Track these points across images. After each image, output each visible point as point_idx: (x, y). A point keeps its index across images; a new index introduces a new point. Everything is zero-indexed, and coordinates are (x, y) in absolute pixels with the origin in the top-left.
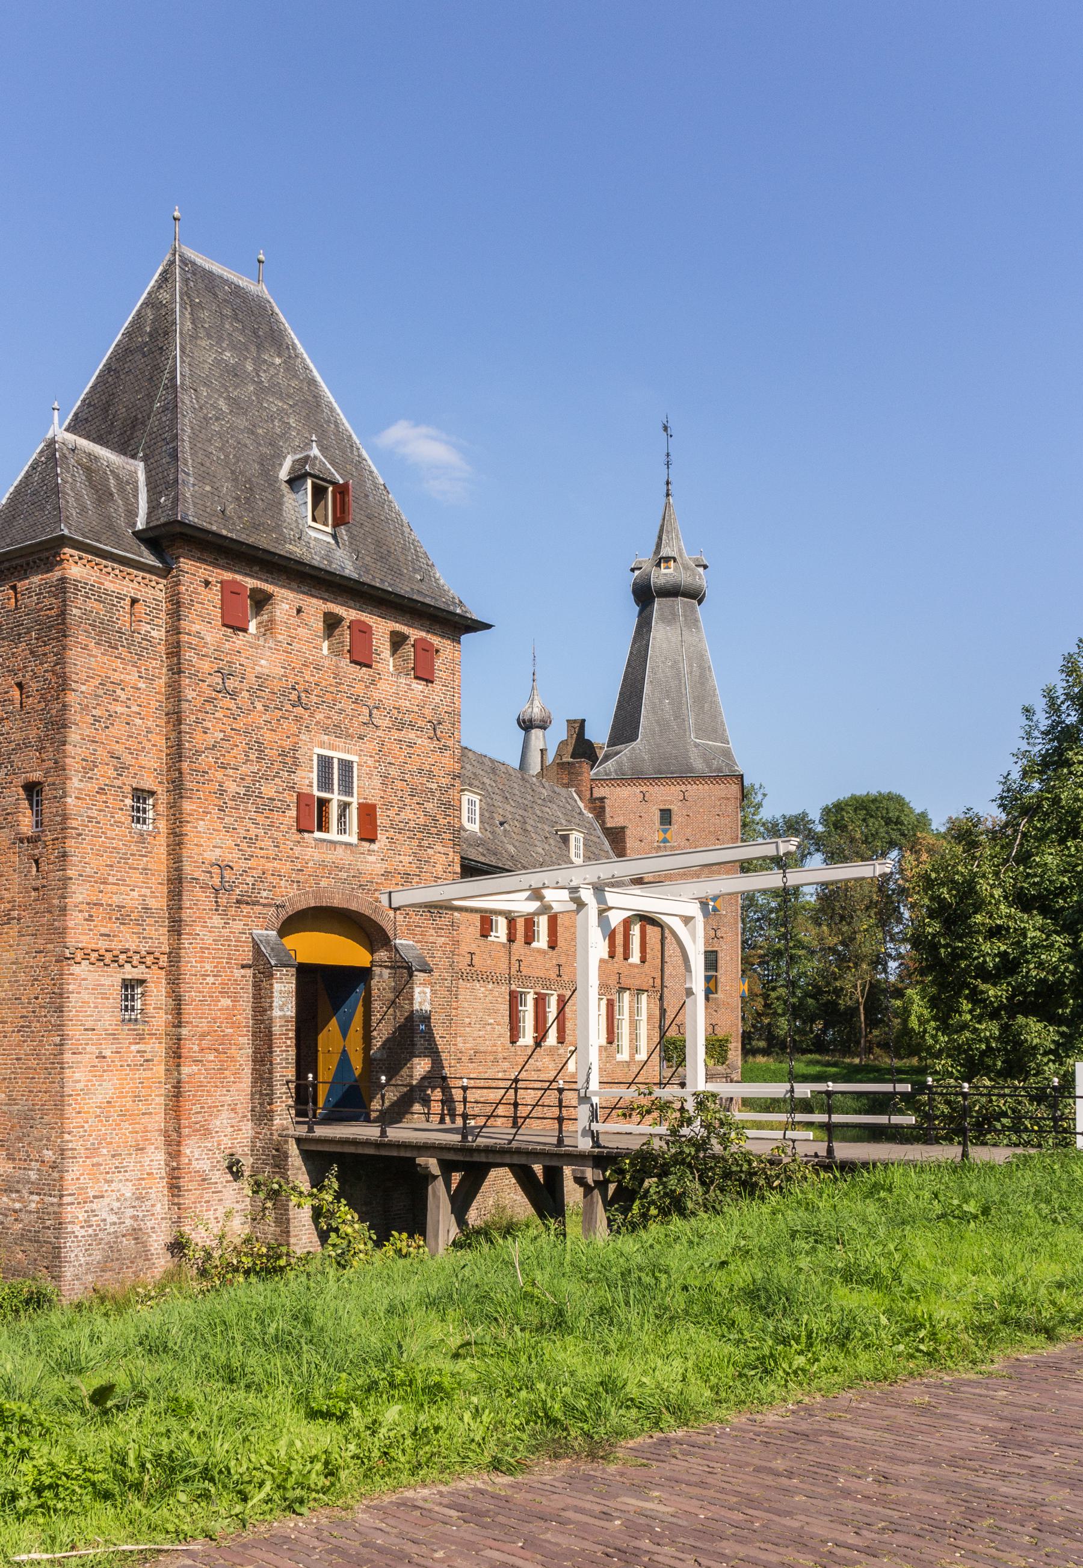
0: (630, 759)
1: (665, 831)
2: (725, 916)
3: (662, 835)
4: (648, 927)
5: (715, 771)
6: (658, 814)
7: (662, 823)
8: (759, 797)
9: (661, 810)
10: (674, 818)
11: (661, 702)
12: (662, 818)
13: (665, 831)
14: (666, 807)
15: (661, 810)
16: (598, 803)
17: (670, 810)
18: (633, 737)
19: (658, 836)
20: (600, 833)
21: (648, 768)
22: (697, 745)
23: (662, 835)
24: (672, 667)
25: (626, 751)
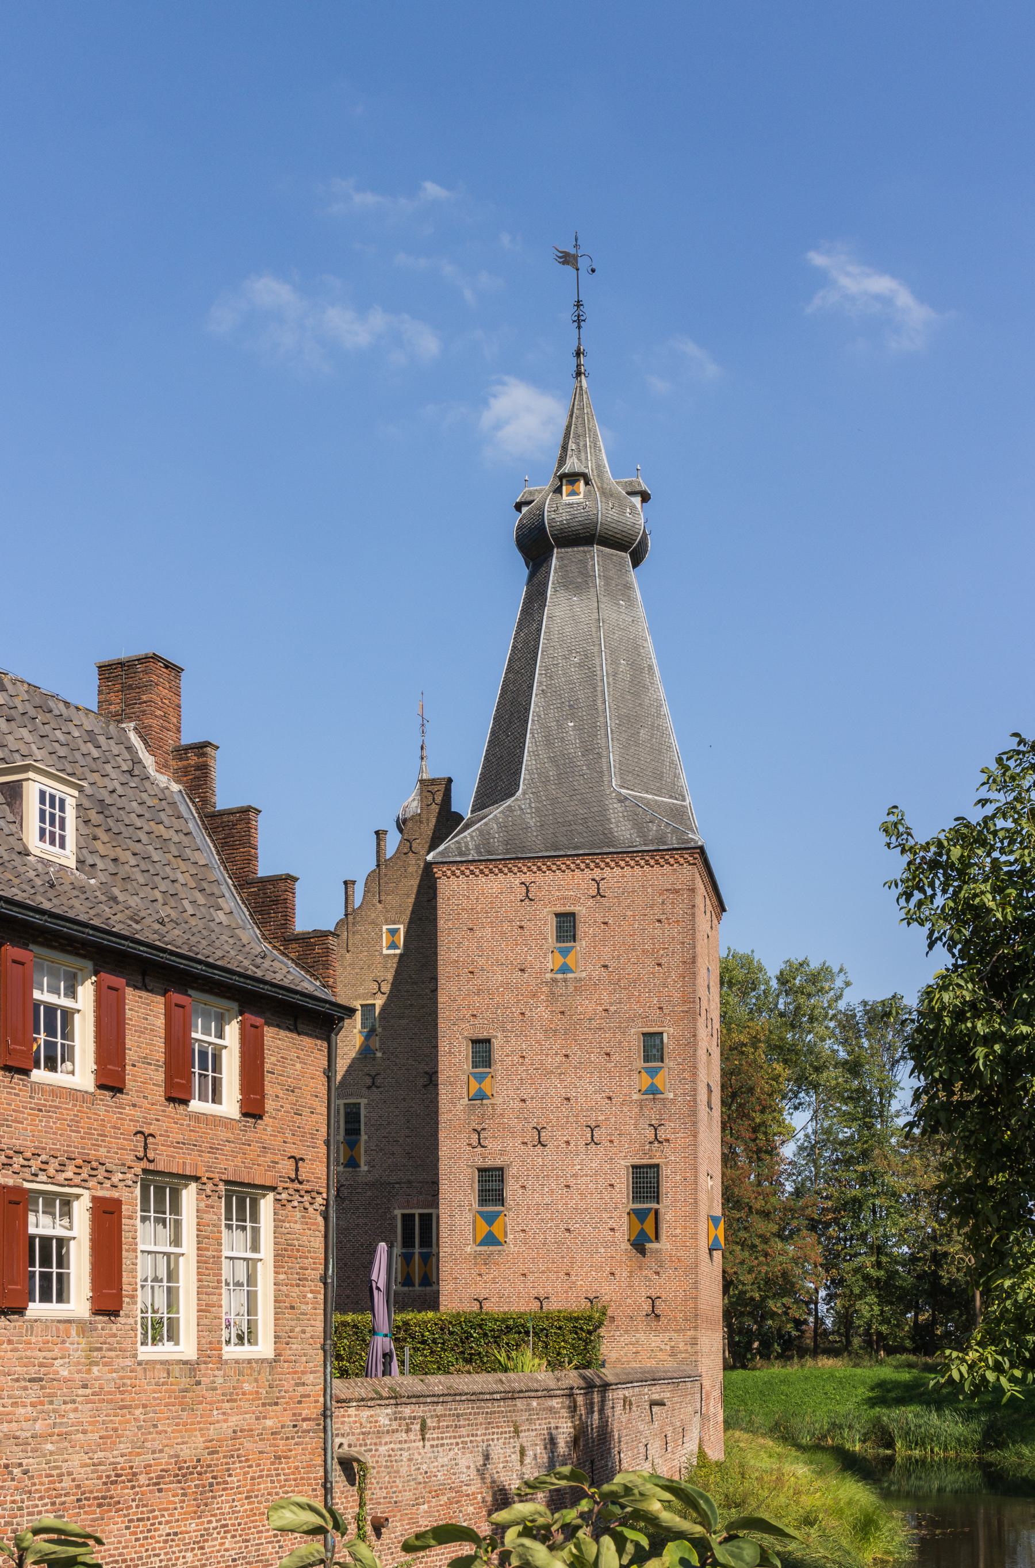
0: (503, 827)
1: (564, 953)
2: (673, 1101)
3: (560, 960)
4: (270, 1034)
5: (652, 842)
6: (552, 922)
7: (560, 938)
8: (839, 983)
9: (557, 915)
10: (581, 929)
11: (560, 726)
12: (559, 928)
13: (564, 953)
14: (568, 909)
15: (557, 915)
16: (193, 759)
17: (573, 915)
18: (510, 791)
19: (552, 962)
20: (194, 826)
21: (535, 841)
22: (622, 799)
23: (560, 960)
24: (580, 665)
25: (496, 812)
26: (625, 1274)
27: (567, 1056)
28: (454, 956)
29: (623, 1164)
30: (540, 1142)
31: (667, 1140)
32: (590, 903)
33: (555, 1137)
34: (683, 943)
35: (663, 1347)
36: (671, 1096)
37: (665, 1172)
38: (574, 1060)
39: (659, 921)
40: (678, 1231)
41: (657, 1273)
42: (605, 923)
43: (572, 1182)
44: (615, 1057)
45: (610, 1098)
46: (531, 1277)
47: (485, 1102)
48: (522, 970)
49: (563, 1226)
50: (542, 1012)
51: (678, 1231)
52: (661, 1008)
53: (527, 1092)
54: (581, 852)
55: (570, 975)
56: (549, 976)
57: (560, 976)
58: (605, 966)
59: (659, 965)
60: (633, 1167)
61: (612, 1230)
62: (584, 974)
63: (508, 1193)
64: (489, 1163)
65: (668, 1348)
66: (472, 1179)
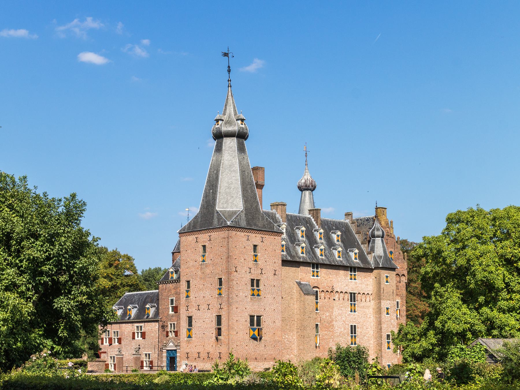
26: (215, 346)
36: (223, 296)
37: (222, 317)
38: (205, 286)
40: (225, 334)
41: (221, 346)
43: (205, 320)
44: (213, 285)
46: (197, 347)
47: (189, 298)
48: (196, 261)
49: (203, 333)
50: (199, 273)
51: (225, 334)
53: (196, 295)
54: (205, 229)
55: (205, 263)
56: (201, 263)
57: (203, 263)
58: (211, 260)
60: (217, 316)
62: (207, 262)
63: (193, 323)
64: (190, 315)
66: (186, 320)
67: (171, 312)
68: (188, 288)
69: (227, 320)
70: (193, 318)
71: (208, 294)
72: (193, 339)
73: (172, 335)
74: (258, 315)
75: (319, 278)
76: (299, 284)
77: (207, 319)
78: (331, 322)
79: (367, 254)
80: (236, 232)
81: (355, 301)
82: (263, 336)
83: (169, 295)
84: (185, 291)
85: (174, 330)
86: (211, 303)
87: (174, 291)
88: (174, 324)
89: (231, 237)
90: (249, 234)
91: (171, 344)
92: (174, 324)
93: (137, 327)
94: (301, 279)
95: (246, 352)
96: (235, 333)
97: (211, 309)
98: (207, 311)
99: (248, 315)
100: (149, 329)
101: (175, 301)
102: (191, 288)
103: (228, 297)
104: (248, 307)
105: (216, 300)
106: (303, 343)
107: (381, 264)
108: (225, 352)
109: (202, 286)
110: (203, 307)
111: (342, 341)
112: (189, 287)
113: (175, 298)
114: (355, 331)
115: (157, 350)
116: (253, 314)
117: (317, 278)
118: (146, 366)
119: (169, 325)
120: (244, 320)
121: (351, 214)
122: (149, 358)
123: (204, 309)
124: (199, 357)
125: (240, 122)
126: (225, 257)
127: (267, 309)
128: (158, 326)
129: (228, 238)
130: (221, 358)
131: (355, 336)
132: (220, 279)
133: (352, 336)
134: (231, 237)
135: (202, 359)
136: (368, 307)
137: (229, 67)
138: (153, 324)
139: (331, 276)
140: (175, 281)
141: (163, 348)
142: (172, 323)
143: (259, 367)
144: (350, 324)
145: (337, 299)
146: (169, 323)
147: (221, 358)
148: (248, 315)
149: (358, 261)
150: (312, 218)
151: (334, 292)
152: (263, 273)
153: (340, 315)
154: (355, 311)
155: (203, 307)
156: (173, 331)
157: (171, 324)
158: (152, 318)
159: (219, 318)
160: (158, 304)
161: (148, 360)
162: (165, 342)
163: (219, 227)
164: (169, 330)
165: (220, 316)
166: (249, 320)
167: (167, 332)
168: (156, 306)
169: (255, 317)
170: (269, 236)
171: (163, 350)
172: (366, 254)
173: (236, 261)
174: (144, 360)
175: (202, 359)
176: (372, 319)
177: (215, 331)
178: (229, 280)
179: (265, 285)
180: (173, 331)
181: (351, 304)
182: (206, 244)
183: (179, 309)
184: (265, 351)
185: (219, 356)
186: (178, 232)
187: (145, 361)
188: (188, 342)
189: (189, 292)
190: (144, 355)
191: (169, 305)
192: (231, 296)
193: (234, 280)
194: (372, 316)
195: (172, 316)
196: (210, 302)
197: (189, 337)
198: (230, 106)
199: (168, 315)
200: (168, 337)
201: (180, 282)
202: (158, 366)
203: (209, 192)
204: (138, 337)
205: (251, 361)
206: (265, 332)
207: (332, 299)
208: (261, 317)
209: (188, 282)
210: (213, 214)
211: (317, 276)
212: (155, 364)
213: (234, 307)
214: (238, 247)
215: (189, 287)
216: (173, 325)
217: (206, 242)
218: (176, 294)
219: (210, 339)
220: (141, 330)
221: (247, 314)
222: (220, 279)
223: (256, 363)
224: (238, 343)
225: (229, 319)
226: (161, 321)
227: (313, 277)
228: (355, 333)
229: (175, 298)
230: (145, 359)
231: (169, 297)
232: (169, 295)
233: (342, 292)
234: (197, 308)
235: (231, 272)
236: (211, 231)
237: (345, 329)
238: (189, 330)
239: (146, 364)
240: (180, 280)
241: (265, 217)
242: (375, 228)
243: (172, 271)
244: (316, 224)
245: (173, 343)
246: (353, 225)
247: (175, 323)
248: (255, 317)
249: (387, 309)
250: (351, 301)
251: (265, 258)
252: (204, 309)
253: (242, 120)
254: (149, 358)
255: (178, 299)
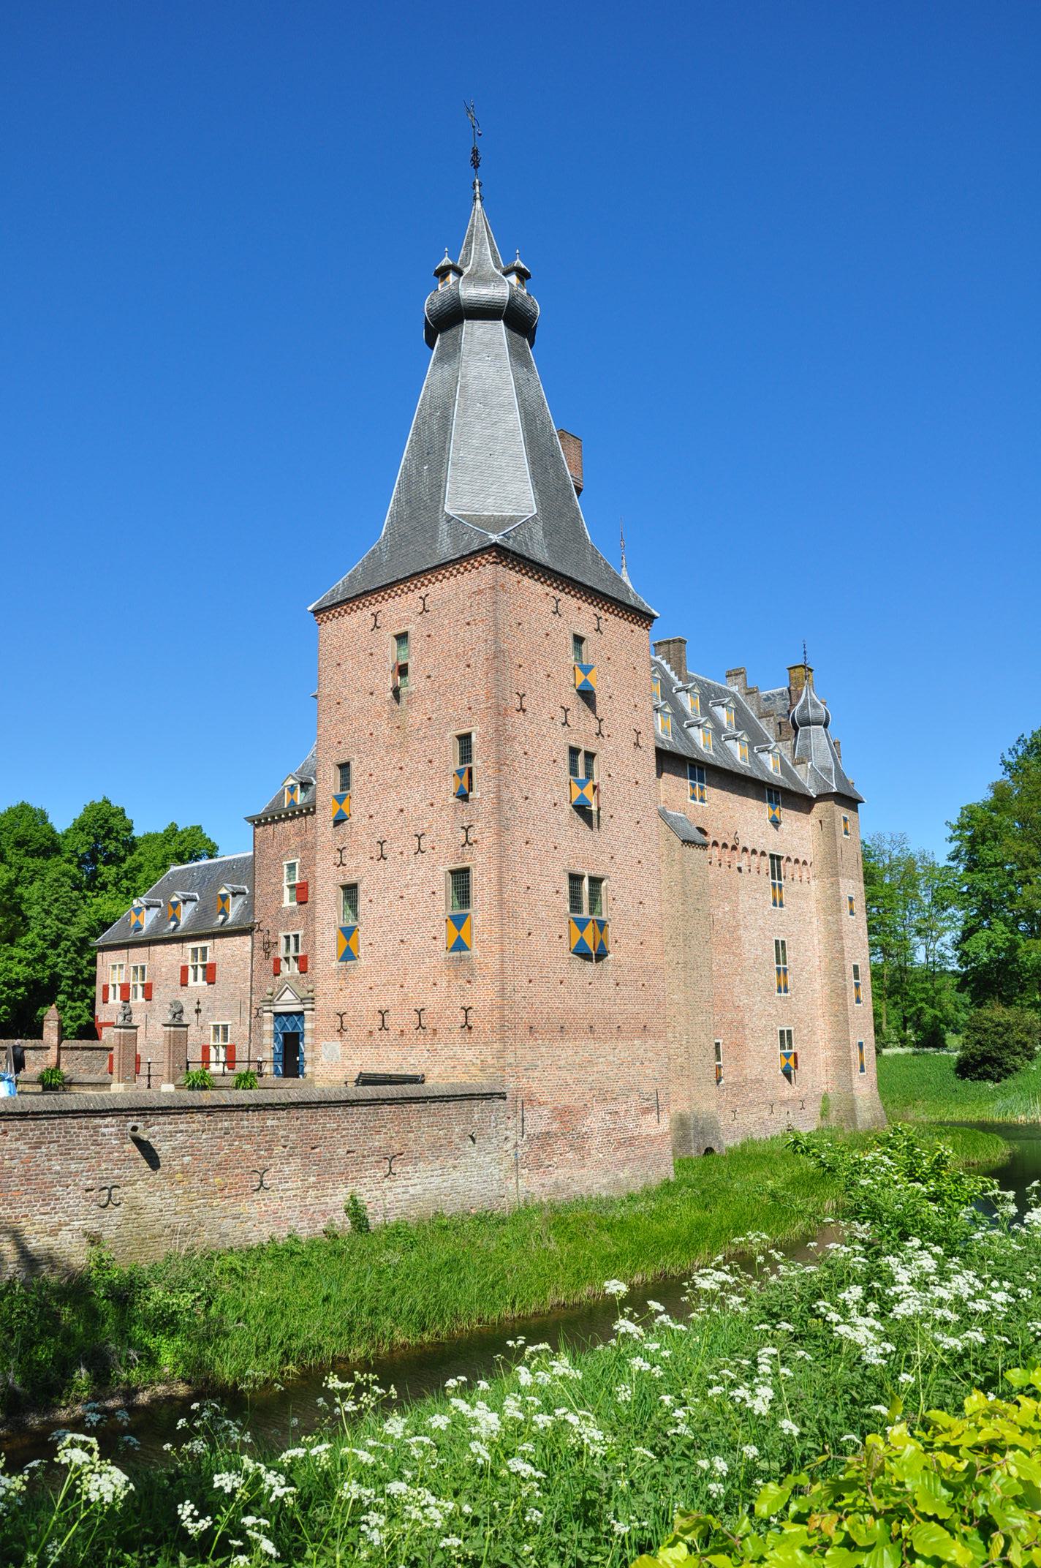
27: (401, 768)
28: (327, 691)
29: (443, 869)
30: (382, 856)
31: (476, 842)
32: (419, 619)
33: (391, 849)
34: (486, 641)
35: (474, 1061)
37: (474, 874)
39: (468, 624)
40: (486, 936)
41: (469, 982)
42: (429, 636)
44: (436, 764)
45: (432, 805)
46: (376, 991)
48: (372, 694)
52: (470, 708)
58: (429, 677)
59: (468, 666)
60: (452, 872)
61: (435, 938)
62: (414, 687)
64: (350, 880)
65: (479, 1062)
67: (288, 902)
68: (342, 790)
69: (495, 882)
70: (361, 888)
71: (418, 797)
72: (362, 962)
73: (289, 970)
74: (593, 874)
75: (706, 805)
76: (663, 815)
77: (412, 890)
78: (736, 927)
79: (794, 764)
80: (519, 576)
81: (780, 879)
82: (610, 948)
83: (283, 852)
84: (332, 800)
85: (297, 954)
86: (430, 826)
87: (298, 839)
88: (296, 937)
89: (503, 586)
90: (559, 595)
91: (288, 996)
92: (296, 937)
93: (195, 950)
94: (665, 802)
95: (561, 1006)
96: (523, 934)
97: (429, 851)
98: (412, 857)
99: (564, 871)
100: (225, 955)
101: (301, 870)
102: (354, 786)
103: (499, 797)
104: (563, 845)
105: (448, 814)
106: (682, 984)
107: (834, 785)
108: (488, 1003)
109: (396, 772)
110: (401, 844)
111: (761, 984)
112: (346, 784)
113: (298, 860)
114: (784, 954)
115: (246, 1015)
116: (578, 870)
117: (701, 804)
118: (217, 1062)
119: (283, 941)
120: (551, 888)
121: (742, 673)
122: (225, 1039)
123: (401, 853)
124: (383, 1027)
125: (513, 279)
126: (483, 657)
127: (619, 857)
128: (250, 944)
129: (493, 588)
130: (470, 1028)
131: (785, 970)
132: (465, 739)
133: (778, 970)
134: (503, 586)
135: (394, 1033)
136: (805, 896)
137: (475, 152)
138: (237, 940)
139: (731, 806)
140: (301, 811)
141: (266, 1008)
142: (291, 933)
143: (601, 1060)
144: (774, 938)
145: (745, 869)
146: (281, 935)
147: (470, 1028)
148: (564, 871)
149: (779, 775)
150: (664, 662)
151: (740, 848)
152: (605, 732)
153: (752, 911)
154: (781, 905)
155: (401, 844)
156: (295, 958)
157: (287, 937)
158: (233, 924)
159: (461, 878)
160: (253, 889)
161: (221, 1043)
162: (269, 990)
163: (458, 556)
164: (281, 954)
165: (466, 871)
166: (568, 889)
167: (277, 961)
168: (247, 892)
169: (586, 881)
170: (617, 618)
171: (265, 1014)
172: (790, 764)
173: (522, 677)
174: (212, 1043)
175: (394, 1033)
176: (815, 927)
177: (444, 928)
178: (501, 737)
179: (610, 776)
180: (295, 958)
181: (774, 885)
182: (410, 628)
183: (310, 892)
184: (618, 1001)
185: (462, 1019)
186: (310, 608)
187: (215, 1046)
188: (345, 975)
189: (347, 800)
190: (212, 1030)
191: (281, 882)
192: (506, 796)
193: (514, 738)
194: (814, 920)
195: (292, 912)
196: (426, 825)
197: (348, 955)
198: (482, 243)
199: (280, 910)
200: (278, 975)
201: (314, 813)
202: (249, 1062)
203: (419, 473)
204: (196, 979)
205: (575, 1039)
206: (617, 935)
207: (734, 868)
208: (604, 884)
209: (344, 767)
210: (435, 528)
211: (702, 800)
212: (241, 1055)
213: (518, 835)
214: (526, 626)
215: (346, 784)
216: (292, 940)
217: (409, 620)
218: (303, 847)
219: (427, 960)
220: (204, 958)
221: (559, 868)
222: (465, 739)
223: (591, 1044)
224: (535, 973)
225: (501, 878)
226: (259, 930)
227: (693, 802)
228: (785, 963)
229: (298, 860)
230: (215, 1040)
231: (281, 859)
232: (283, 852)
233: (754, 852)
234: (376, 854)
235: (505, 710)
236: (430, 581)
237: (764, 951)
238: (348, 932)
239: (218, 1054)
240: (314, 807)
241: (602, 558)
242: (806, 701)
243: (292, 786)
244: (676, 678)
245: (294, 993)
246: (750, 697)
247: (301, 933)
248: (586, 881)
249: (851, 899)
250: (773, 878)
251: (608, 687)
252: (401, 853)
253: (523, 275)
254: (225, 1039)
255: (309, 864)
